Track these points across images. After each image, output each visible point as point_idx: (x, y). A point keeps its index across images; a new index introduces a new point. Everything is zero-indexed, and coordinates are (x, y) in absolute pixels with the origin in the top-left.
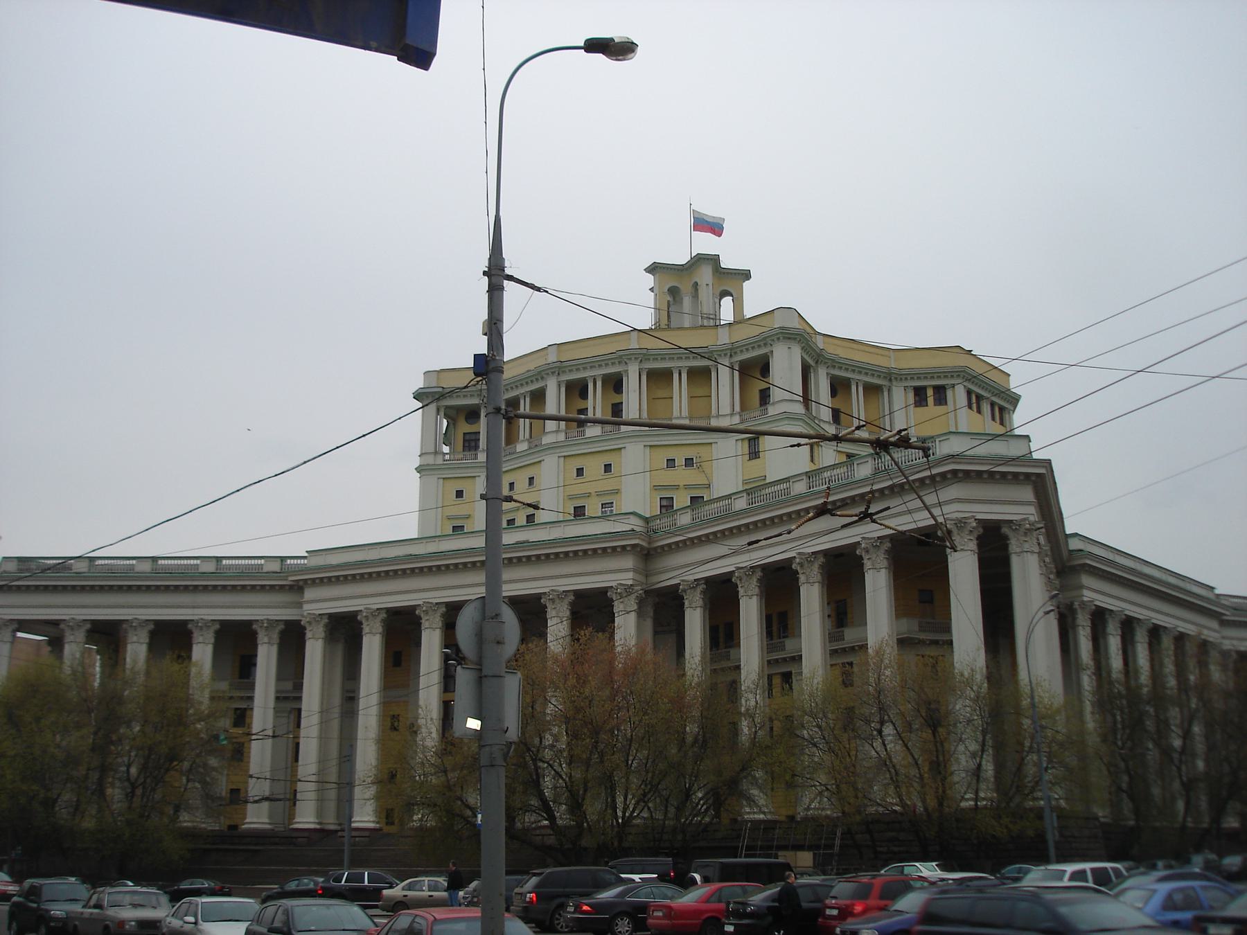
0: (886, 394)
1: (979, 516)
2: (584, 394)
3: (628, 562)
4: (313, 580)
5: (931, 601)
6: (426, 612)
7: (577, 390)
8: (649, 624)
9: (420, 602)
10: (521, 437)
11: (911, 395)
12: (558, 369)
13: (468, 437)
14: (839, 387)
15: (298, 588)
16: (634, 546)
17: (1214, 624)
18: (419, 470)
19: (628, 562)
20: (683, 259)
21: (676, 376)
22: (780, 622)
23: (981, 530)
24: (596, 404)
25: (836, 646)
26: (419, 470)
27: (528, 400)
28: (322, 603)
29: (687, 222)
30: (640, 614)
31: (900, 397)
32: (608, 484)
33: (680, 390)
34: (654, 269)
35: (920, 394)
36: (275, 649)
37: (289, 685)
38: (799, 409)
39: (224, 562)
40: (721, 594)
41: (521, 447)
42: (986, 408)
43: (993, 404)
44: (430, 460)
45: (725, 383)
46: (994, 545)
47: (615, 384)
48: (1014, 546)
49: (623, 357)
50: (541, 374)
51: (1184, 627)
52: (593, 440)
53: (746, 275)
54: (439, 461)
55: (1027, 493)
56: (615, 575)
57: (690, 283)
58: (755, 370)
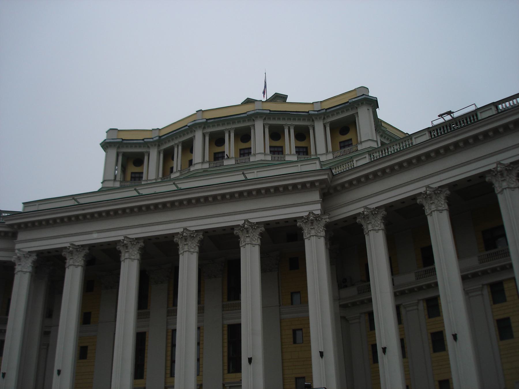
3: (316, 196)
4: (26, 224)
6: (126, 246)
16: (321, 181)
24: (230, 147)
27: (180, 148)
47: (244, 136)
56: (303, 207)
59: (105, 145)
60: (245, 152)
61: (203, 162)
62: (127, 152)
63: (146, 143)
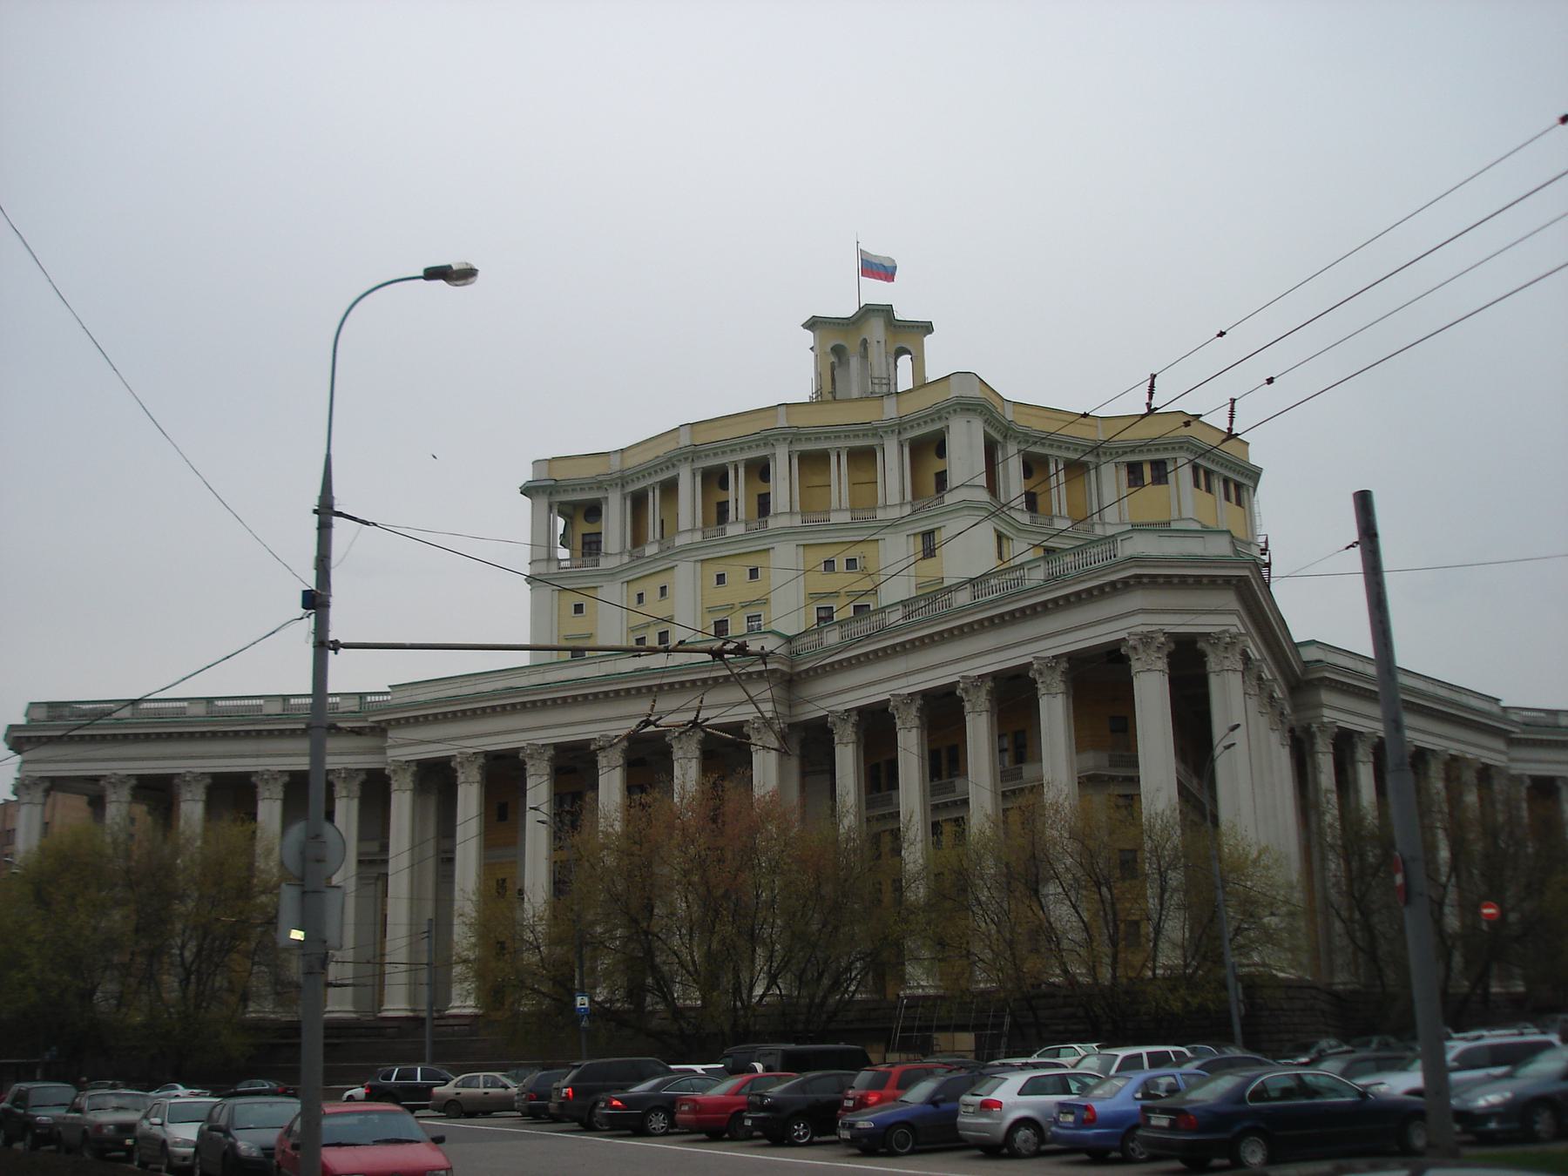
0: (1093, 472)
1: (1167, 629)
2: (724, 484)
4: (398, 720)
6: (531, 757)
7: (715, 479)
8: (794, 764)
9: (523, 744)
10: (651, 538)
11: (1124, 473)
12: (692, 454)
13: (588, 539)
14: (1033, 466)
15: (380, 730)
17: (1500, 745)
20: (848, 310)
21: (834, 459)
22: (945, 761)
23: (1173, 646)
24: (738, 494)
25: (1011, 786)
28: (407, 748)
29: (854, 265)
30: (783, 753)
31: (1111, 479)
32: (752, 591)
33: (839, 476)
34: (813, 324)
35: (1134, 470)
36: (355, 804)
37: (374, 847)
38: (984, 496)
39: (292, 701)
40: (876, 726)
41: (651, 550)
42: (1218, 486)
43: (1226, 481)
44: (542, 568)
45: (893, 464)
46: (1188, 665)
47: (760, 470)
48: (1212, 663)
50: (671, 461)
51: (1455, 749)
52: (737, 540)
53: (927, 328)
54: (554, 568)
55: (1229, 600)
58: (928, 448)
59: (527, 491)
60: (763, 505)
61: (692, 530)
63: (598, 484)
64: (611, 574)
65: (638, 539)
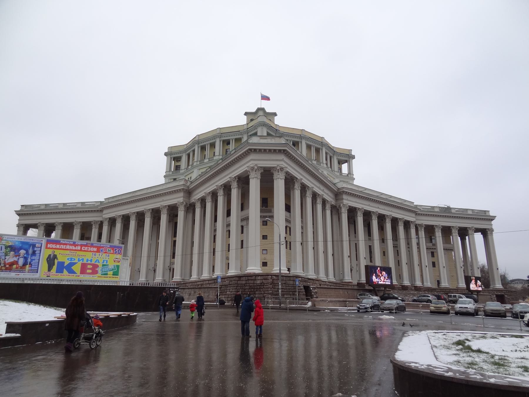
3: (182, 194)
5: (267, 203)
7: (203, 148)
15: (101, 211)
16: (183, 189)
17: (414, 215)
18: (165, 177)
19: (182, 194)
20: (254, 110)
26: (165, 177)
28: (109, 214)
34: (246, 114)
41: (190, 167)
44: (168, 173)
49: (214, 137)
56: (178, 199)
57: (261, 119)
59: (166, 154)
62: (175, 156)
63: (181, 152)
64: (183, 174)
65: (188, 165)
